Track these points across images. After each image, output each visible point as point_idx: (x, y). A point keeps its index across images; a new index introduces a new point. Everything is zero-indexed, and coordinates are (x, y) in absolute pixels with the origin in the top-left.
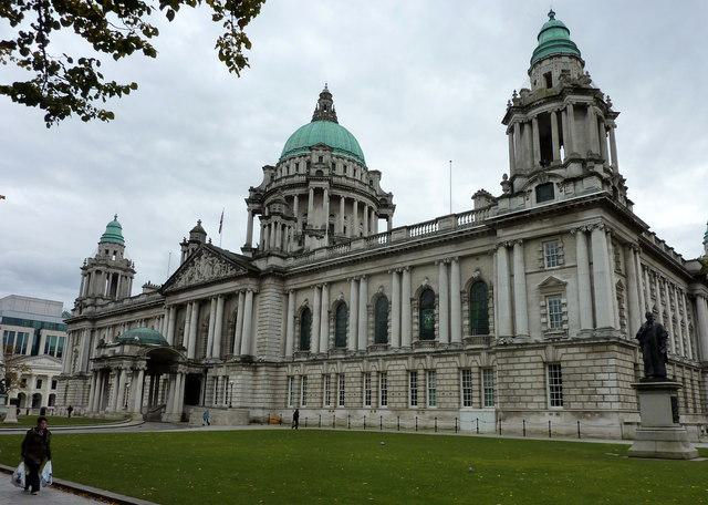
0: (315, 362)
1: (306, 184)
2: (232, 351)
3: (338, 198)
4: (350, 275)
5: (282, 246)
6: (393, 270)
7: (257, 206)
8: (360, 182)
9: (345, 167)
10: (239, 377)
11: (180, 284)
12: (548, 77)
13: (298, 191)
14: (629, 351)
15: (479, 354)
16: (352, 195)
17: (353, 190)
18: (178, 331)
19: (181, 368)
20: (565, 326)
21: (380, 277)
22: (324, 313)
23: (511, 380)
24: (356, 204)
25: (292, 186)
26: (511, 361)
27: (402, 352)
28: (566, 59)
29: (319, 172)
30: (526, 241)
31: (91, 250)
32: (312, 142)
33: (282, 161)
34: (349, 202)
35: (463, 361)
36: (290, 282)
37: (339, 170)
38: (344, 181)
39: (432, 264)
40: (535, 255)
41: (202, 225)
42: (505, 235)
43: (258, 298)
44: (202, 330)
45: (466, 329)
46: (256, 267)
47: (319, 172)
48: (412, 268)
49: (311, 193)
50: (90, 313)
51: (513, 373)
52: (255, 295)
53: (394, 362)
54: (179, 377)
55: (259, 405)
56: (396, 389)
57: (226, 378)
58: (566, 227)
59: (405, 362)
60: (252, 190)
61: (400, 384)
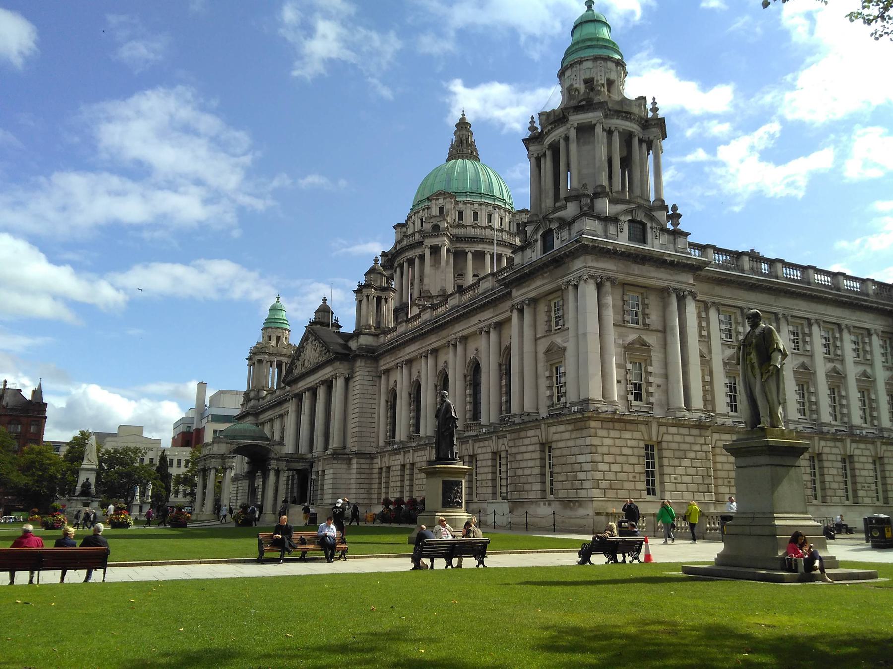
0: (396, 452)
1: (420, 244)
9: (476, 214)
11: (297, 372)
13: (417, 252)
14: (629, 426)
16: (481, 247)
17: (481, 240)
19: (273, 464)
22: (405, 395)
24: (488, 257)
28: (589, 64)
31: (255, 337)
33: (409, 217)
34: (479, 256)
36: (382, 362)
37: (468, 219)
38: (472, 232)
41: (328, 303)
42: (519, 295)
43: (351, 384)
47: (436, 228)
49: (427, 252)
50: (252, 408)
51: (519, 457)
52: (347, 380)
54: (272, 475)
58: (561, 282)
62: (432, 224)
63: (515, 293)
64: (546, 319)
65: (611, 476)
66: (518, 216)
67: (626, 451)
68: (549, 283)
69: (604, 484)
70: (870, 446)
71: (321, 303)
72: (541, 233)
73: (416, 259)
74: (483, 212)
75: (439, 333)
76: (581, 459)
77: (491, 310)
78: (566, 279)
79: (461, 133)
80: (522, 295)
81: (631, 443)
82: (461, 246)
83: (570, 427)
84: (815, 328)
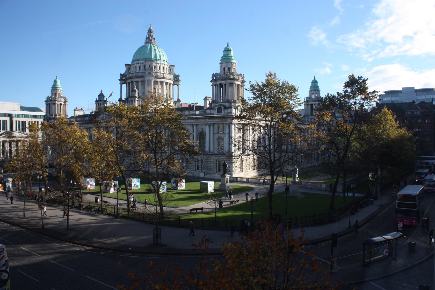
3: (157, 82)
12: (224, 69)
13: (140, 79)
17: (163, 78)
26: (209, 159)
41: (103, 92)
51: (209, 162)
60: (121, 75)
62: (148, 72)
63: (207, 120)
71: (100, 92)
72: (217, 107)
73: (140, 82)
80: (210, 122)
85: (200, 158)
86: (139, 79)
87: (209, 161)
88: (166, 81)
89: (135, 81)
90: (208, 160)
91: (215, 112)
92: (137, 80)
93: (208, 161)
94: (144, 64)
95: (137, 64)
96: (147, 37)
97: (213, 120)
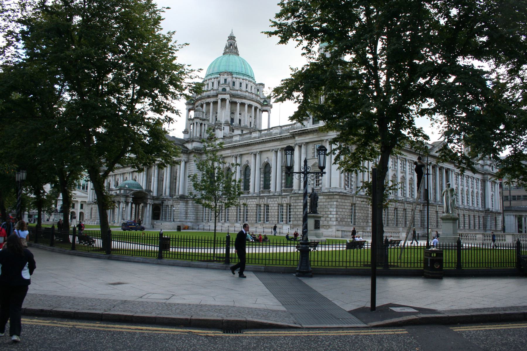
2: (175, 193)
3: (236, 103)
4: (233, 154)
5: (200, 135)
6: (252, 153)
7: (191, 107)
8: (251, 93)
9: (241, 84)
10: (179, 206)
14: (347, 198)
15: (287, 197)
16: (244, 101)
17: (245, 98)
18: (149, 181)
19: (149, 201)
20: (320, 186)
21: (247, 156)
23: (296, 210)
24: (246, 106)
25: (209, 97)
26: (297, 201)
27: (255, 195)
29: (224, 90)
30: (307, 144)
32: (222, 69)
35: (279, 200)
37: (237, 86)
38: (239, 93)
39: (269, 150)
40: (312, 150)
42: (299, 140)
43: (188, 165)
44: (160, 180)
45: (283, 185)
46: (186, 148)
47: (224, 90)
48: (261, 152)
49: (219, 101)
52: (186, 163)
53: (251, 200)
54: (148, 206)
55: (188, 220)
56: (252, 214)
57: (172, 206)
58: (323, 138)
59: (256, 200)
61: (253, 211)
62: (222, 88)
63: (297, 138)
64: (313, 152)
65: (341, 216)
66: (258, 86)
67: (346, 207)
68: (317, 138)
69: (339, 219)
70: (411, 205)
74: (244, 83)
75: (245, 148)
76: (332, 209)
77: (279, 142)
78: (326, 138)
79: (231, 41)
81: (348, 204)
82: (239, 101)
83: (326, 197)
84: (399, 160)
85: (285, 202)
86: (210, 99)
87: (298, 206)
88: (248, 103)
89: (205, 102)
90: (296, 203)
91: (309, 124)
92: (208, 100)
93: (297, 204)
94: (219, 79)
95: (209, 80)
96: (226, 46)
97: (305, 137)
